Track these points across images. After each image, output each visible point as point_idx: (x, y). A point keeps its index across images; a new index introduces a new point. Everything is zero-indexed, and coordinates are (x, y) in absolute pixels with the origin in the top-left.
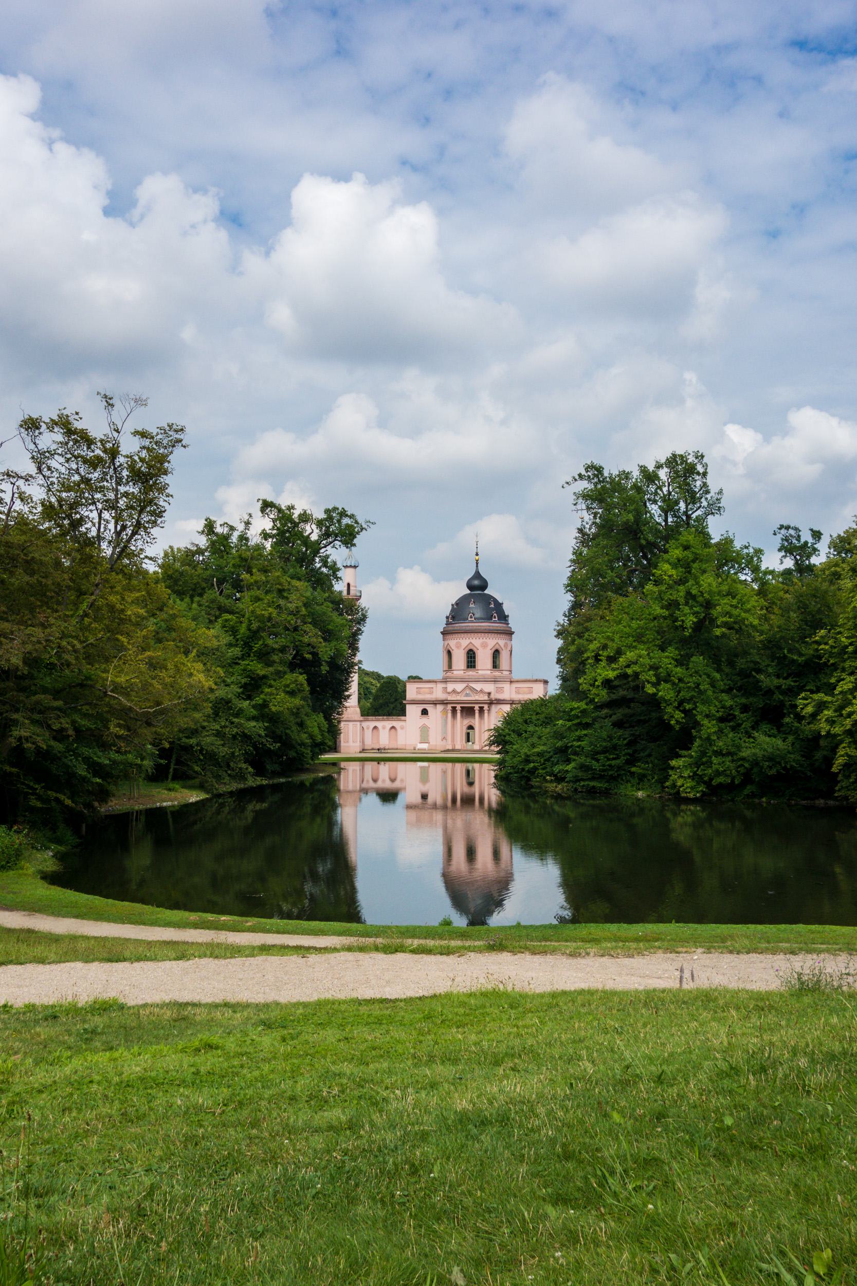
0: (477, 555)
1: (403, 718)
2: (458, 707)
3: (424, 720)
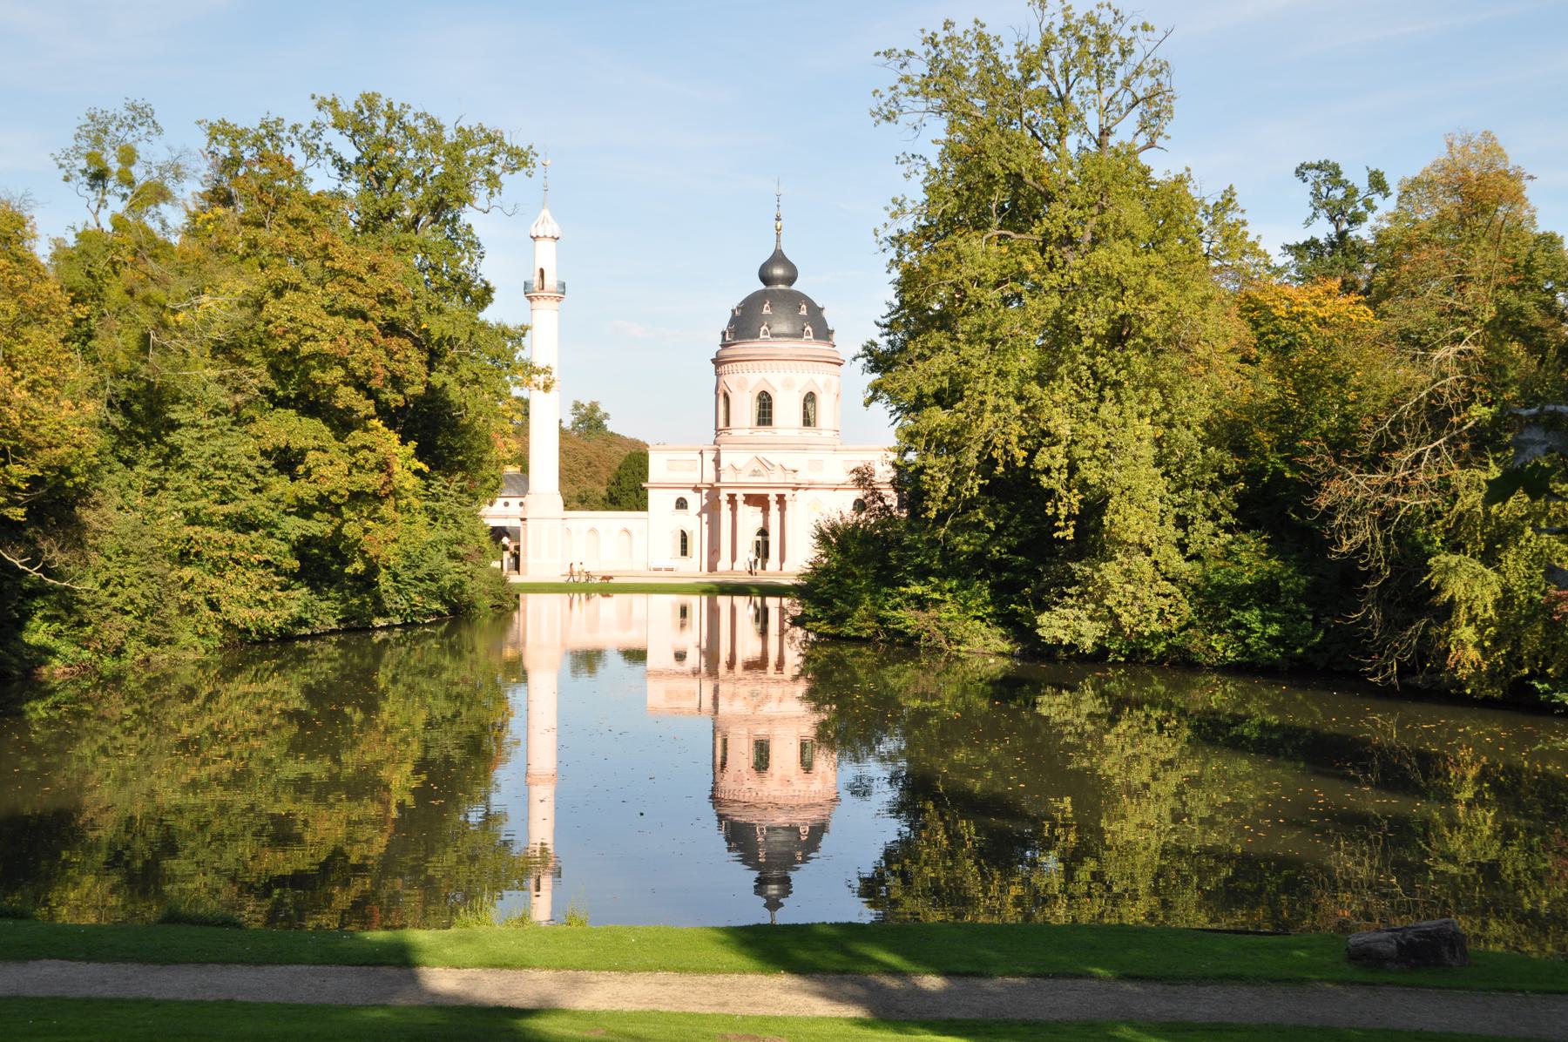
0: (778, 219)
2: (740, 498)
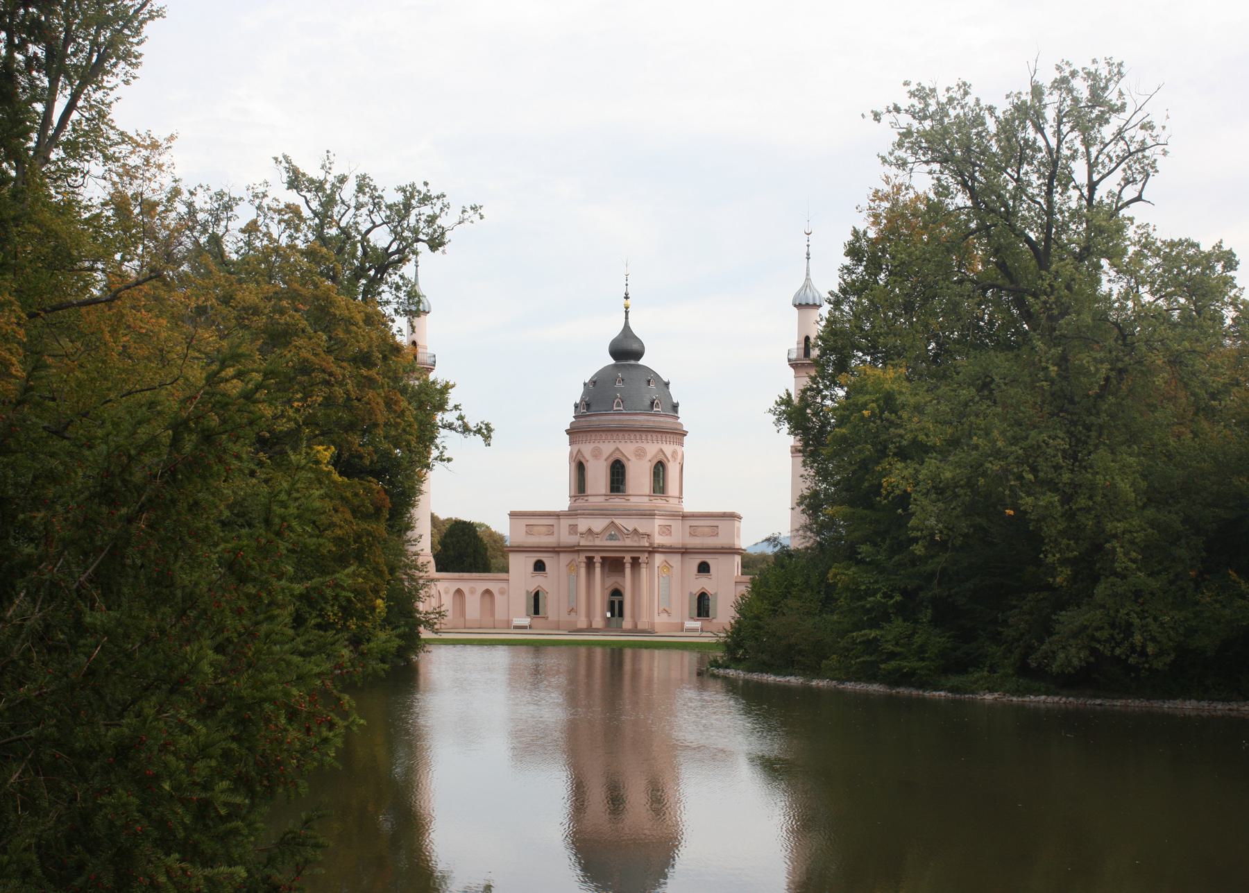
1: (503, 575)
2: (597, 559)
3: (538, 581)
